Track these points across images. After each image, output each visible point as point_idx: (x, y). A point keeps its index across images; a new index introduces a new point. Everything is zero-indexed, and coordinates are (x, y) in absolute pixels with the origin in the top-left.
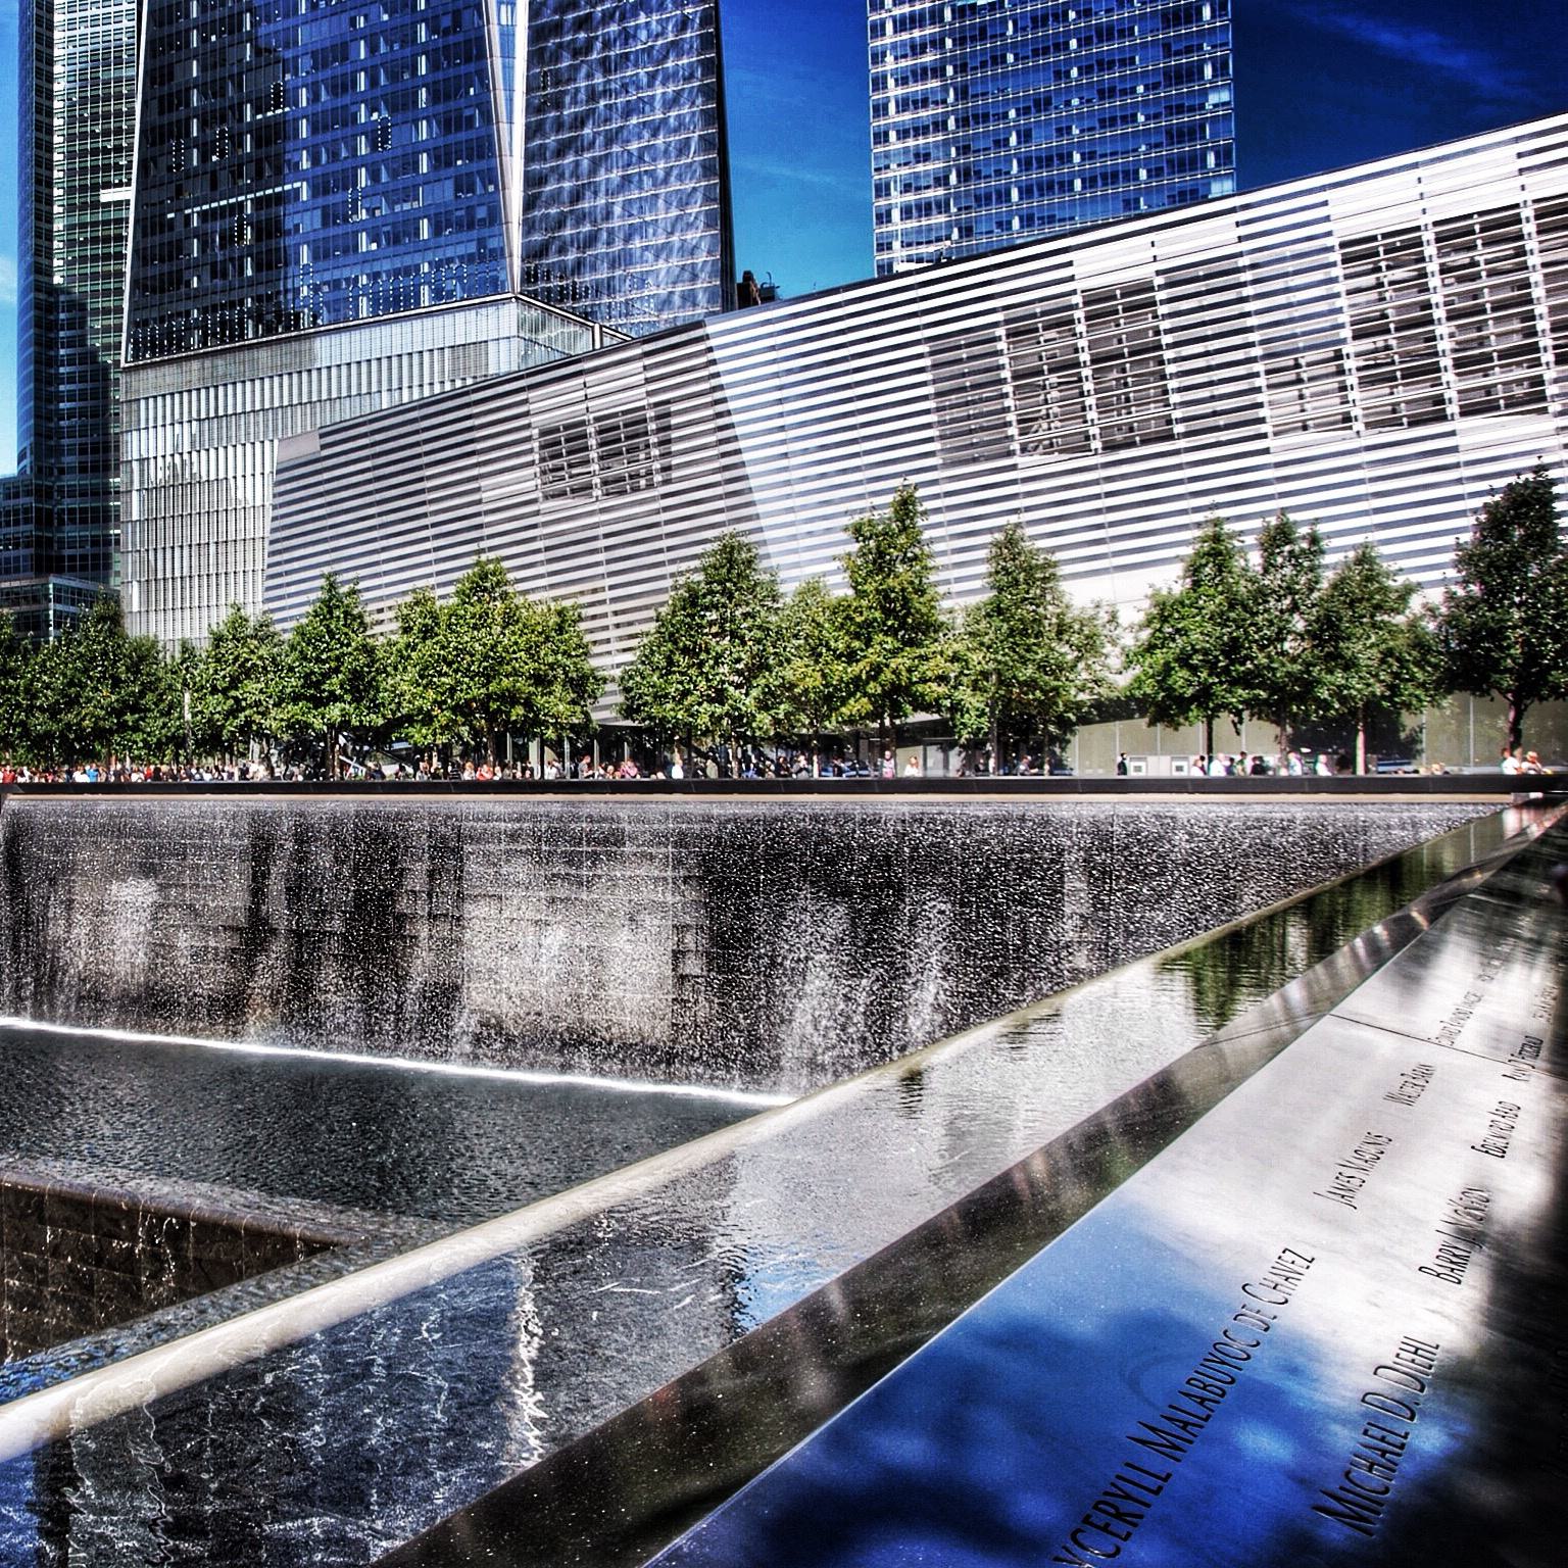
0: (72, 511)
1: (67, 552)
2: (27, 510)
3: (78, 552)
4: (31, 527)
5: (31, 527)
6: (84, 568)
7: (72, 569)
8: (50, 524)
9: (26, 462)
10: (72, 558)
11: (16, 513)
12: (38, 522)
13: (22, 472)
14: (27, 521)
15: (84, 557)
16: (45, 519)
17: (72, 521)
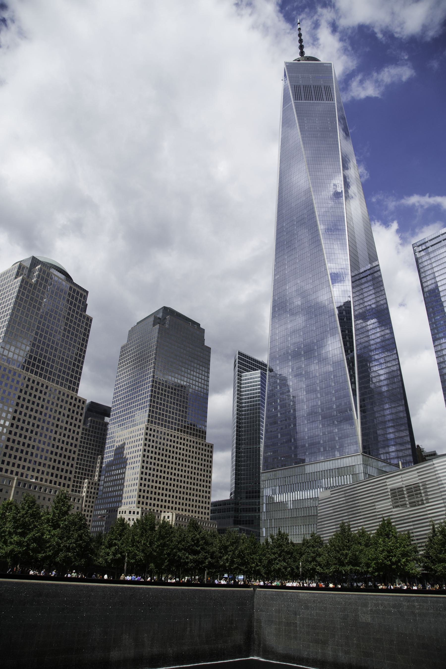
0: (243, 509)
1: (242, 519)
2: (232, 508)
3: (245, 519)
4: (233, 512)
5: (233, 512)
6: (246, 524)
7: (243, 524)
8: (238, 511)
9: (232, 495)
10: (243, 521)
11: (230, 508)
12: (235, 511)
13: (231, 498)
14: (232, 511)
15: (246, 521)
16: (236, 510)
17: (244, 511)
